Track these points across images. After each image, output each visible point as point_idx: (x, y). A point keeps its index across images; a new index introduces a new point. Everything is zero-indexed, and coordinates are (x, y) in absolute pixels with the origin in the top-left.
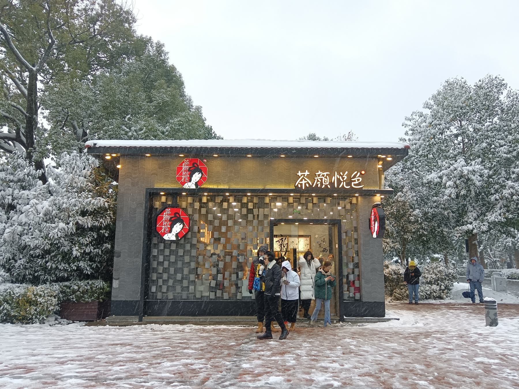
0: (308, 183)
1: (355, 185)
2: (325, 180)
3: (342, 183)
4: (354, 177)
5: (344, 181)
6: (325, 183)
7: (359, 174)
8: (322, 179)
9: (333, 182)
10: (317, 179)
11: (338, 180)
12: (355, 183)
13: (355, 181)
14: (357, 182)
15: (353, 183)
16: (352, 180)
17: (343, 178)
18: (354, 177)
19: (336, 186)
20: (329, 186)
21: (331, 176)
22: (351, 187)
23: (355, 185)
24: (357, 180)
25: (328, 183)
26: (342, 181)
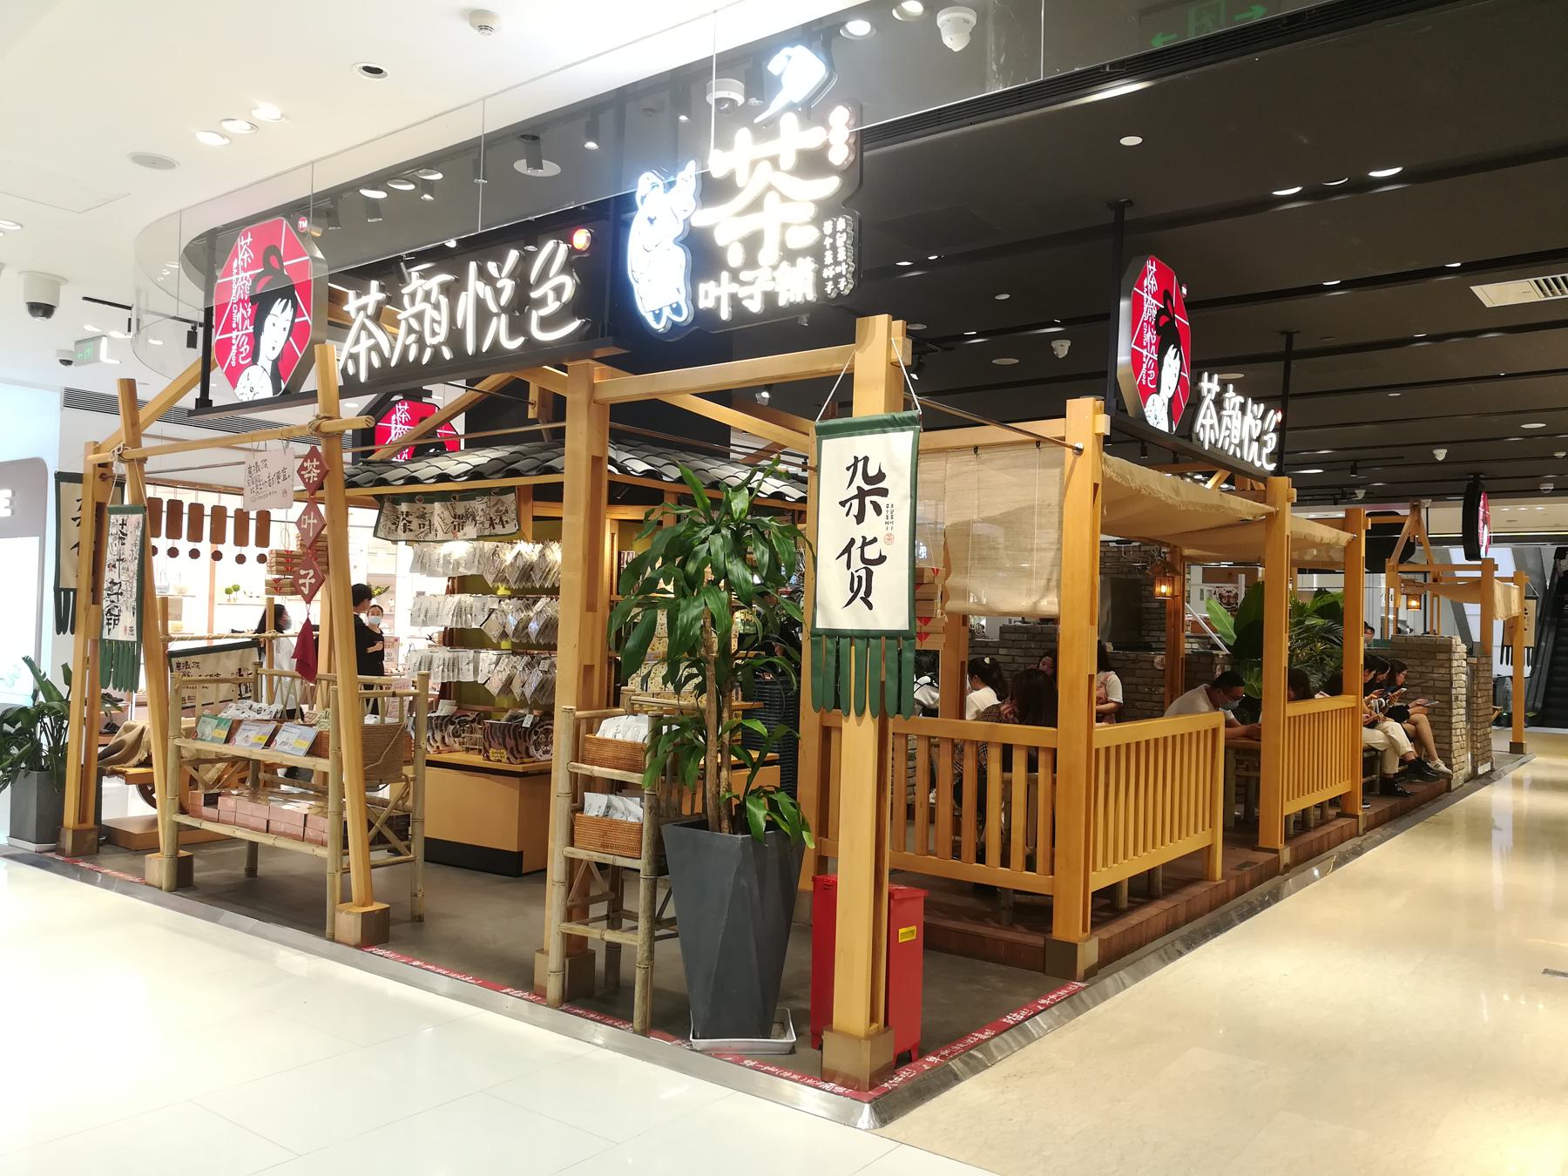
0: (376, 348)
1: (547, 323)
3: (495, 319)
4: (544, 276)
5: (498, 315)
6: (434, 334)
7: (563, 248)
8: (419, 317)
9: (459, 325)
10: (406, 319)
11: (480, 304)
12: (544, 312)
13: (542, 302)
14: (552, 306)
15: (535, 316)
16: (534, 295)
17: (497, 293)
19: (470, 349)
20: (447, 354)
21: (451, 292)
22: (530, 342)
23: (547, 323)
24: (551, 296)
25: (441, 338)
26: (493, 308)
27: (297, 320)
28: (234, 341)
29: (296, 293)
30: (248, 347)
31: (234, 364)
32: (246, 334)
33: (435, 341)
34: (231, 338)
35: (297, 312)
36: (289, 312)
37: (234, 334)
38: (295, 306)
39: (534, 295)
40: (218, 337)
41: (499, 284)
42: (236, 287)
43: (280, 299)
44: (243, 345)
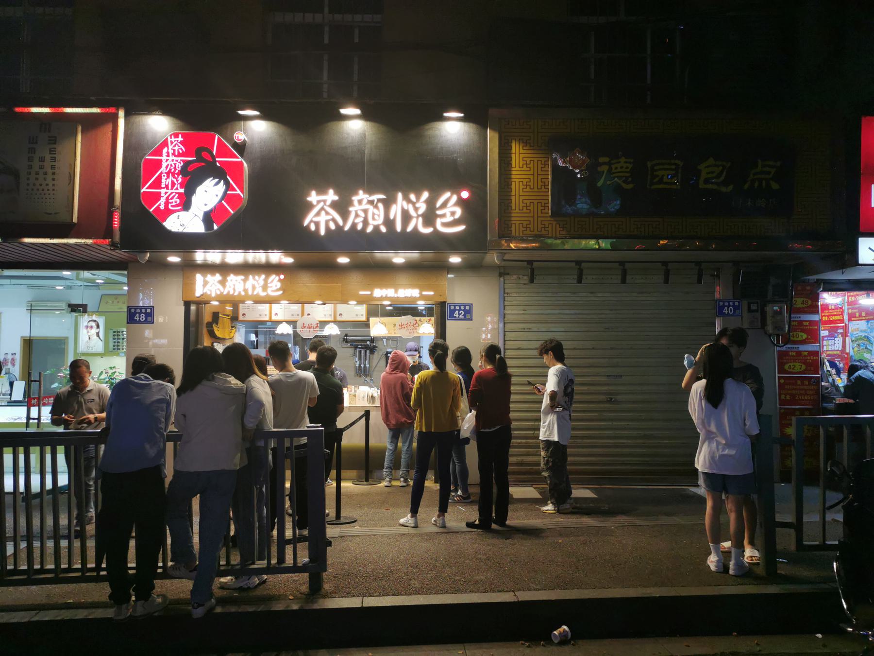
2: (374, 214)
18: (444, 205)
27: (229, 192)
28: (162, 195)
29: (228, 177)
30: (178, 201)
31: (162, 207)
32: (176, 193)
33: (376, 223)
34: (160, 193)
35: (229, 187)
36: (221, 187)
37: (163, 191)
38: (227, 183)
39: (439, 212)
40: (144, 190)
41: (417, 205)
42: (166, 164)
43: (212, 178)
44: (172, 198)
